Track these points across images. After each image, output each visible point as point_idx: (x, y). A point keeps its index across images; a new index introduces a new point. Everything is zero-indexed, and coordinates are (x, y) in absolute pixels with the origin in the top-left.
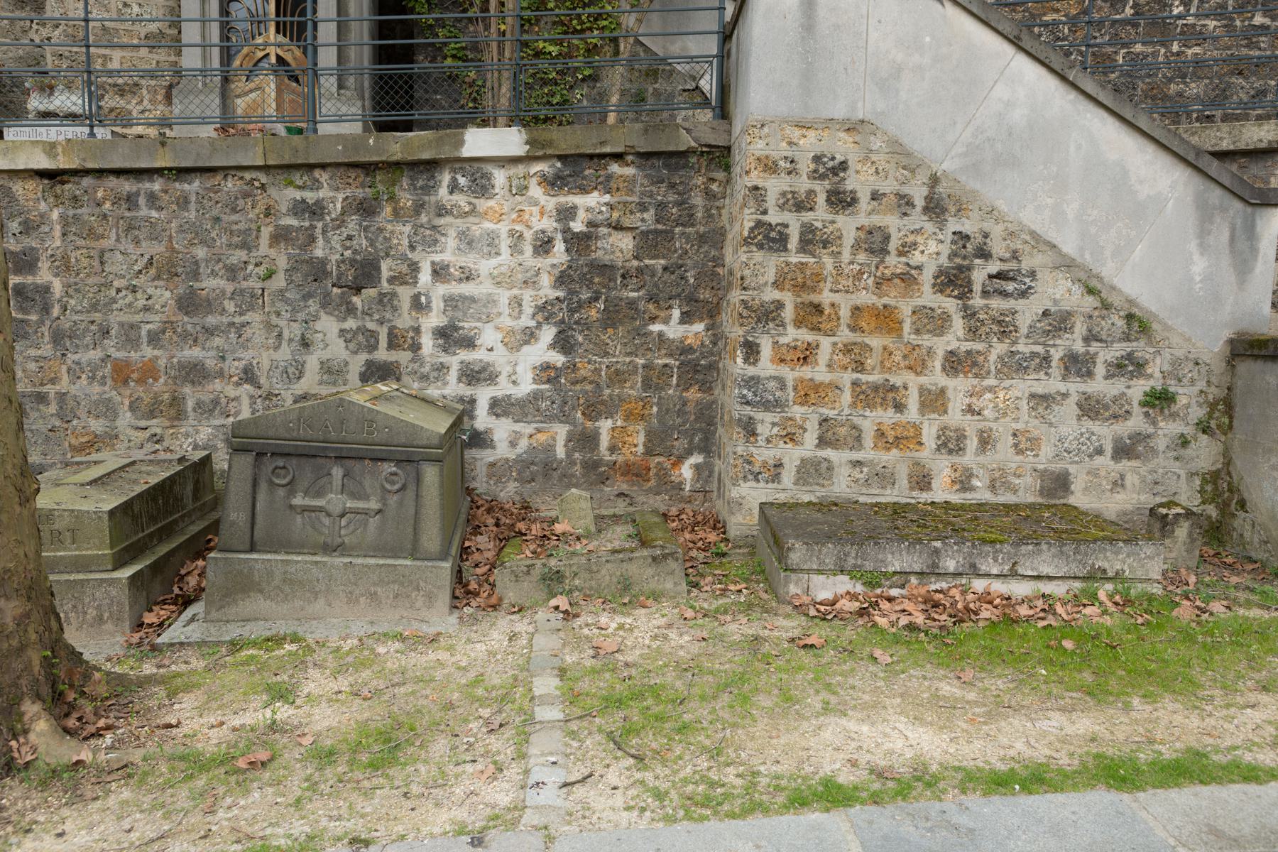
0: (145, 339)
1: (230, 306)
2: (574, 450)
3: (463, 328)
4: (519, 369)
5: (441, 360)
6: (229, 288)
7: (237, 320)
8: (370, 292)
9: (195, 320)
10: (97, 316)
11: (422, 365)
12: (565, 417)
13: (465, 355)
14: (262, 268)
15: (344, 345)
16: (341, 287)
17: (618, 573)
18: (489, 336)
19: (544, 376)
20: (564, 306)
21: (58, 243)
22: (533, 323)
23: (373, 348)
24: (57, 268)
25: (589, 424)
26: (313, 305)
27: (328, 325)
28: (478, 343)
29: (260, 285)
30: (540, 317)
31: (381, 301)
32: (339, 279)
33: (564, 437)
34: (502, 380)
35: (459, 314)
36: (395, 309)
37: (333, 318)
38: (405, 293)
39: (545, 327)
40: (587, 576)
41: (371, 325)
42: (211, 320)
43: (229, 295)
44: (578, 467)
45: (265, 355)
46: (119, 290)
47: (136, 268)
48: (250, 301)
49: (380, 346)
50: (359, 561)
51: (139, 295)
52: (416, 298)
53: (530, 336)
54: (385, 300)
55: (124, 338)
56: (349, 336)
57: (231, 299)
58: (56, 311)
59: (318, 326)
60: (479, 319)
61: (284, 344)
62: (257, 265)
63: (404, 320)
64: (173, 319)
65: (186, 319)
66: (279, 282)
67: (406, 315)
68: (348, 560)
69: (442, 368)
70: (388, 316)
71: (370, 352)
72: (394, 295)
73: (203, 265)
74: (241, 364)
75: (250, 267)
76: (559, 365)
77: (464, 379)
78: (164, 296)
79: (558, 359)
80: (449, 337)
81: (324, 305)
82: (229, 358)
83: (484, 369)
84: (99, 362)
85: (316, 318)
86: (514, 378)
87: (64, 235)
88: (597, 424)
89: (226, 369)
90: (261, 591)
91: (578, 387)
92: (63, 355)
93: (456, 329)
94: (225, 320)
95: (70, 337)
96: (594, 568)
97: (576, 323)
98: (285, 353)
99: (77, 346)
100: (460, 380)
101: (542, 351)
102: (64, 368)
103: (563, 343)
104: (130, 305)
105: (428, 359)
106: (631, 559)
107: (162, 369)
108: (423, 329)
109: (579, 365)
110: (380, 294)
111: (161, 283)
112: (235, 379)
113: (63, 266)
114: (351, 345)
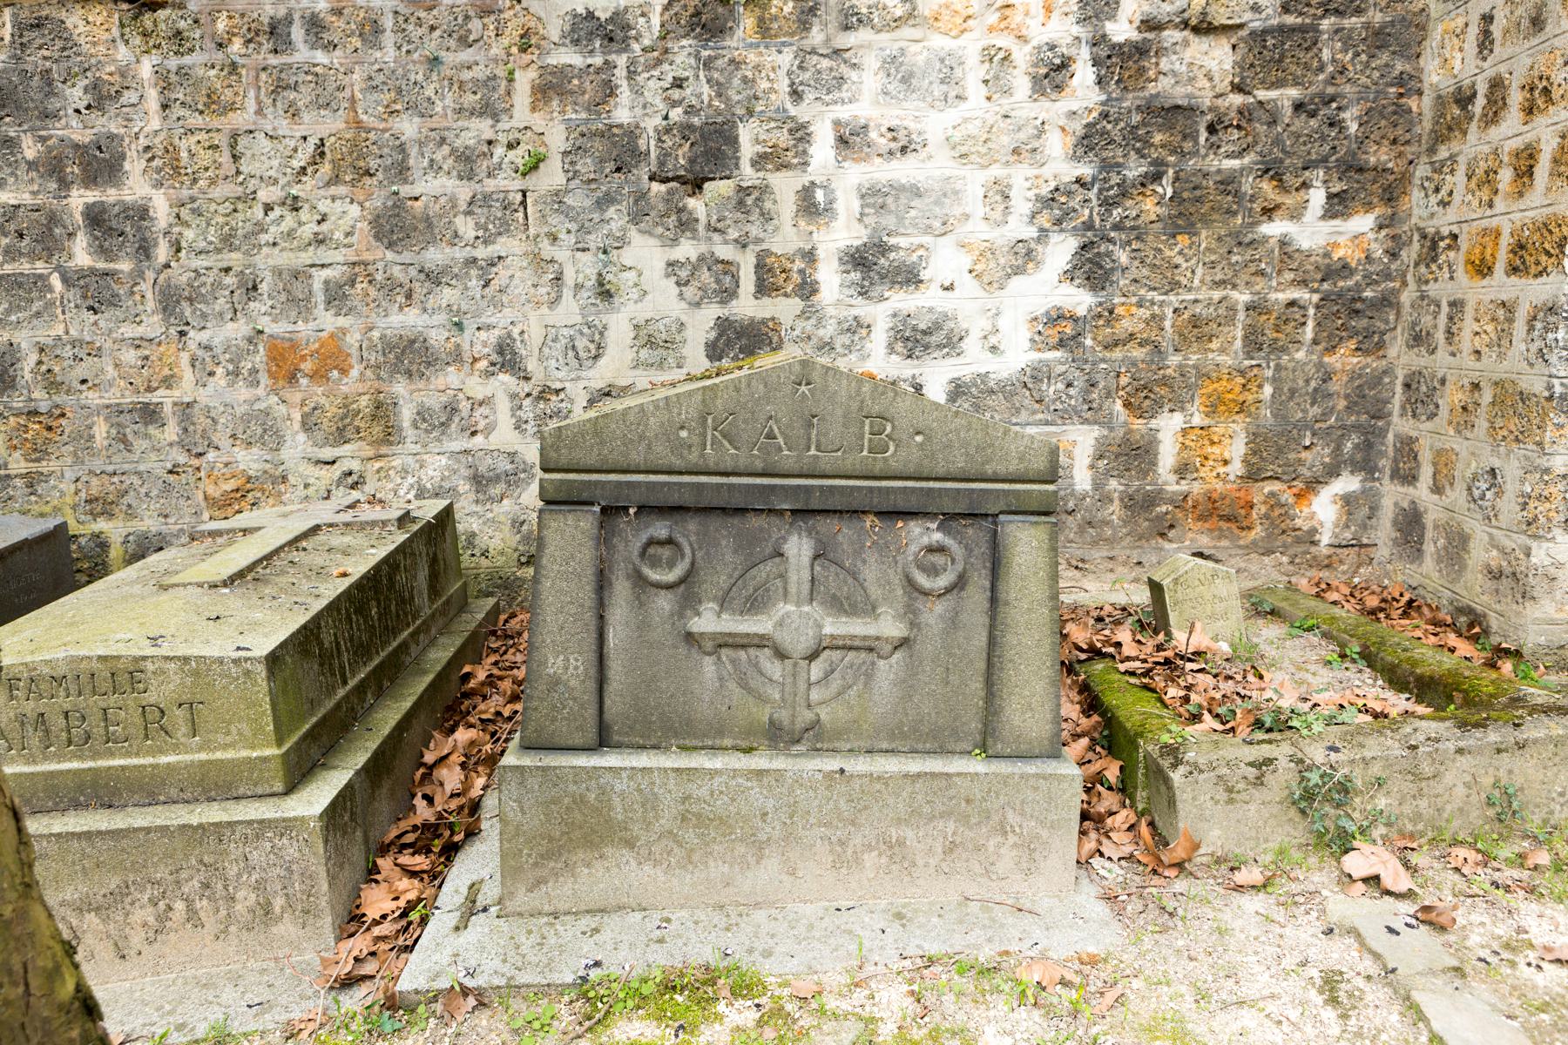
0: (320, 297)
1: (466, 228)
2: (1108, 474)
3: (897, 248)
4: (1002, 323)
5: (855, 312)
6: (464, 192)
7: (482, 253)
8: (718, 189)
9: (407, 257)
10: (234, 259)
11: (819, 324)
12: (1091, 412)
13: (901, 300)
14: (520, 151)
15: (675, 290)
16: (665, 181)
17: (1487, 781)
18: (945, 262)
19: (1053, 334)
20: (1093, 194)
21: (155, 123)
22: (1031, 232)
23: (728, 294)
24: (159, 170)
25: (1138, 424)
26: (616, 217)
27: (646, 254)
28: (924, 275)
29: (518, 184)
30: (1044, 220)
31: (741, 203)
32: (662, 164)
33: (1091, 451)
34: (972, 345)
35: (889, 221)
36: (767, 217)
37: (652, 241)
38: (785, 186)
39: (1055, 238)
40: (1409, 787)
41: (724, 252)
42: (435, 256)
43: (463, 206)
44: (1116, 506)
45: (533, 316)
46: (268, 208)
47: (296, 164)
48: (504, 214)
49: (741, 291)
50: (859, 765)
51: (304, 215)
52: (806, 193)
53: (1025, 257)
54: (749, 201)
55: (283, 297)
56: (684, 274)
57: (468, 213)
58: (162, 252)
59: (627, 256)
60: (928, 230)
61: (567, 293)
62: (510, 146)
63: (785, 239)
64: (367, 256)
65: (390, 255)
66: (552, 176)
67: (788, 229)
68: (832, 764)
69: (858, 327)
70: (754, 231)
71: (723, 302)
72: (765, 189)
73: (413, 151)
74: (492, 337)
75: (499, 151)
76: (1081, 311)
77: (899, 346)
78: (348, 214)
79: (1080, 300)
80: (870, 265)
81: (636, 217)
82: (470, 326)
83: (937, 326)
84: (243, 344)
85: (622, 242)
86: (993, 340)
87: (165, 107)
88: (1154, 423)
89: (466, 346)
90: (630, 844)
91: (1117, 354)
92: (182, 334)
93: (883, 249)
94: (460, 254)
95: (190, 300)
96: (1427, 769)
97: (1117, 227)
98: (569, 311)
99: (204, 316)
100: (891, 349)
101: (1050, 285)
102: (185, 358)
103: (1091, 268)
104: (290, 234)
105: (831, 311)
106: (1521, 746)
107: (354, 352)
108: (821, 253)
109: (1119, 310)
110: (740, 189)
111: (341, 190)
112: (483, 364)
113: (168, 166)
114: (690, 292)
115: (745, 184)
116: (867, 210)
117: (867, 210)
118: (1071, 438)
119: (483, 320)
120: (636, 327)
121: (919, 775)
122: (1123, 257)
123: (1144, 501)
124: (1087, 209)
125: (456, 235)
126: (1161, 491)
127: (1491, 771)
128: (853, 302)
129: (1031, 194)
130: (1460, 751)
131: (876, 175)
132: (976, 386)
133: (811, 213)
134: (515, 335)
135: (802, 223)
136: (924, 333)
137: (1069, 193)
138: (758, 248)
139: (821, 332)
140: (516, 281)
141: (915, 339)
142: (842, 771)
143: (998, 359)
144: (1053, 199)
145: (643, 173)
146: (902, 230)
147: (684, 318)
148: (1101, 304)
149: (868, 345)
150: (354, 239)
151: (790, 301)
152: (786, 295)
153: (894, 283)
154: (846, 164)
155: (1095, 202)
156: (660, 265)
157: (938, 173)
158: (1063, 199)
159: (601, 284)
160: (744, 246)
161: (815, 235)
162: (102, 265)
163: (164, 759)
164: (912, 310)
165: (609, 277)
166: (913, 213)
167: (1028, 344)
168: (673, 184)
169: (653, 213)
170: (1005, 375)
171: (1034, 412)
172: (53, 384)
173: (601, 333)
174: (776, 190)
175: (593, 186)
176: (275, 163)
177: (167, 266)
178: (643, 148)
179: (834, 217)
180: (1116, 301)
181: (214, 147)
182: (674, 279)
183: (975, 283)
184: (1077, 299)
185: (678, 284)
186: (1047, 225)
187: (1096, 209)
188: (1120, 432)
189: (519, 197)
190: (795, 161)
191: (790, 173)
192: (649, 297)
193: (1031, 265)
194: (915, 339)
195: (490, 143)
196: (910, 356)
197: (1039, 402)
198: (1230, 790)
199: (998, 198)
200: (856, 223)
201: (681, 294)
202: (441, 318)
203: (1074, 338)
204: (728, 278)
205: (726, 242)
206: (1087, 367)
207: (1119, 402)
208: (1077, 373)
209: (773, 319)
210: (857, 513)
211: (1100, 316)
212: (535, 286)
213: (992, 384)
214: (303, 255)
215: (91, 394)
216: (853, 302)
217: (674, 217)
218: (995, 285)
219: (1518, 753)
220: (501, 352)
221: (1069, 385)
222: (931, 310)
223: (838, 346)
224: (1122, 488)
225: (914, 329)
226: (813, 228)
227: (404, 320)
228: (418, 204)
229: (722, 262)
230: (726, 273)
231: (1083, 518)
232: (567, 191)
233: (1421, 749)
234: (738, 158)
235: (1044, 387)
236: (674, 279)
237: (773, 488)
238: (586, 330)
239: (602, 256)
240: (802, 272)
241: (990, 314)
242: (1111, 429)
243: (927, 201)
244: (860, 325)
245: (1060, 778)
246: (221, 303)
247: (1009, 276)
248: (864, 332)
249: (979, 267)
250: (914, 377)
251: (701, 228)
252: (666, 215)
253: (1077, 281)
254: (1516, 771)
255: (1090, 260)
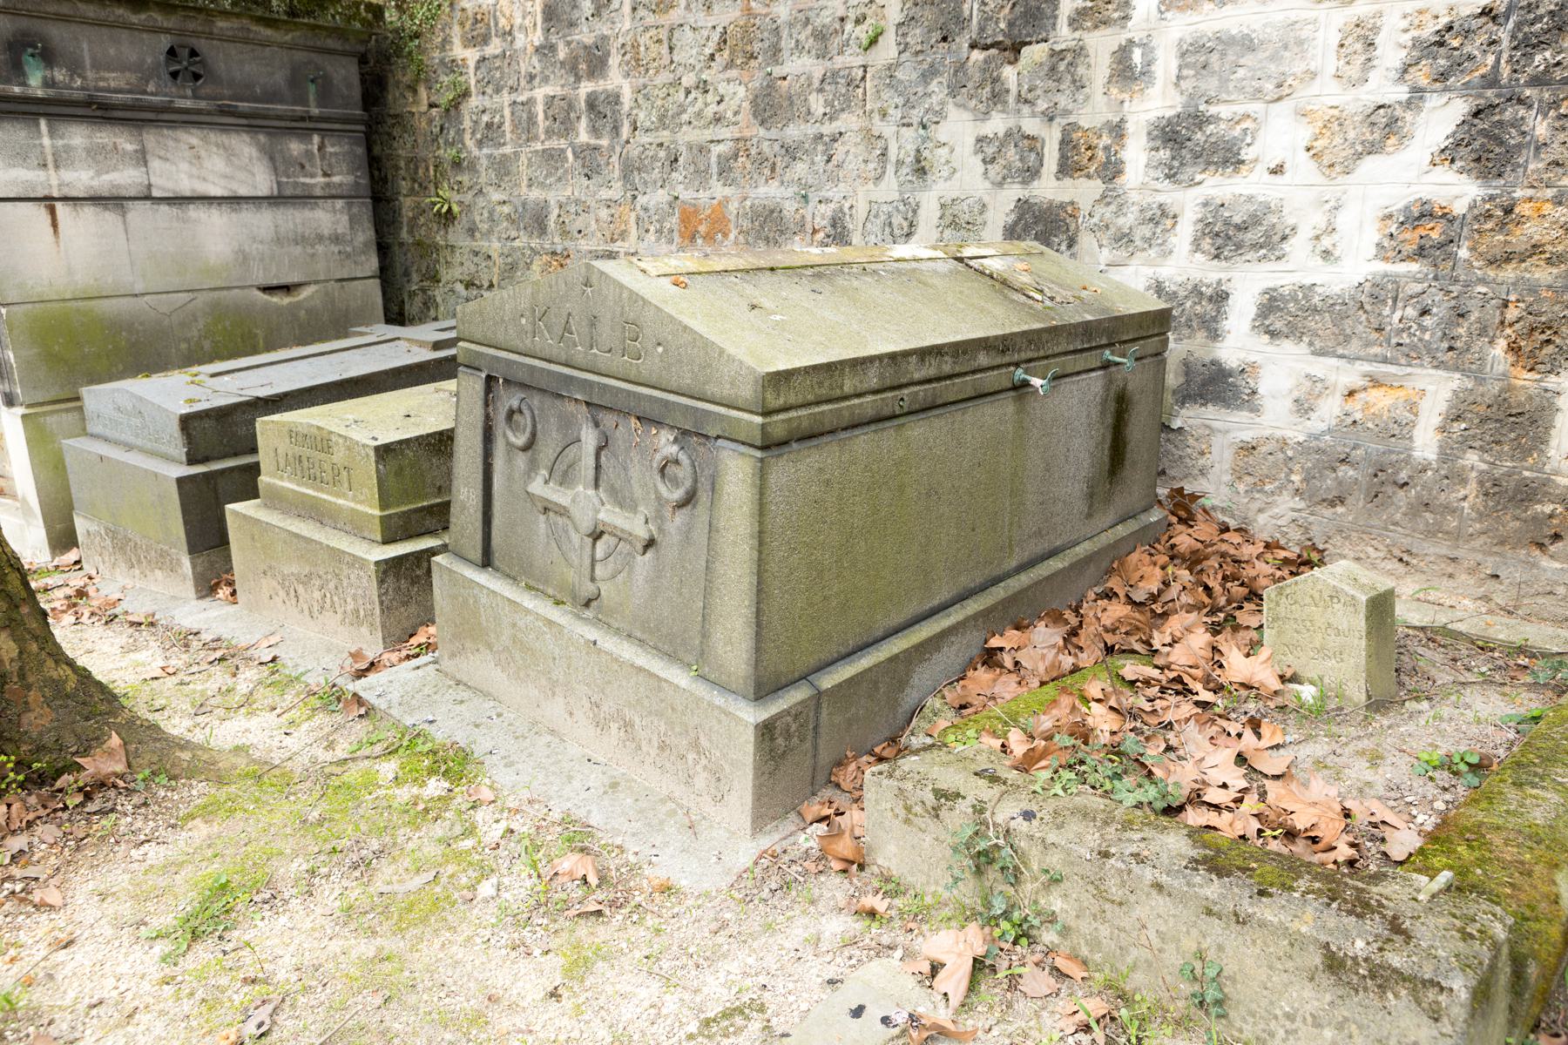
0: (714, 169)
1: (817, 104)
2: (1466, 443)
3: (1216, 119)
4: (1343, 220)
5: (1161, 198)
6: (817, 69)
7: (828, 129)
8: (1034, 53)
9: (774, 133)
10: (664, 136)
11: (1119, 212)
12: (1452, 354)
13: (1217, 186)
14: (864, 27)
15: (980, 168)
16: (986, 48)
17: (1189, 945)
18: (1279, 136)
19: (1411, 237)
20: (1504, 34)
21: (627, 25)
22: (1401, 93)
23: (1031, 174)
24: (628, 63)
25: (1525, 380)
26: (938, 88)
27: (960, 129)
28: (1247, 154)
29: (860, 61)
30: (1421, 76)
31: (1053, 69)
32: (982, 29)
33: (1443, 407)
34: (1298, 248)
35: (1210, 85)
36: (1078, 85)
37: (967, 115)
38: (1101, 44)
39: (1433, 101)
40: (1087, 900)
41: (1031, 126)
42: (795, 132)
43: (816, 84)
44: (1471, 489)
45: (861, 191)
46: (688, 92)
47: (708, 51)
48: (845, 89)
49: (1044, 170)
50: (609, 643)
51: (710, 97)
52: (1122, 53)
53: (1386, 127)
54: (1062, 67)
55: (692, 169)
56: (990, 150)
57: (821, 90)
58: (625, 130)
59: (942, 133)
60: (1257, 94)
61: (890, 169)
62: (858, 22)
63: (1093, 113)
64: (747, 134)
65: (762, 132)
66: (888, 50)
67: (1099, 98)
68: (591, 633)
69: (1161, 217)
70: (1063, 101)
71: (1024, 182)
72: (1079, 52)
73: (785, 34)
74: (827, 210)
75: (849, 27)
76: (1459, 208)
77: (1206, 244)
78: (737, 92)
79: (1460, 191)
80: (1182, 142)
81: (953, 93)
82: (814, 198)
83: (1254, 220)
84: (666, 207)
85: (940, 115)
86: (1326, 242)
87: (634, 9)
88: (1552, 382)
89: (809, 218)
90: (490, 647)
91: (1509, 273)
92: (634, 197)
93: (1200, 121)
94: (811, 130)
95: (639, 170)
96: (1114, 889)
97: (1537, 81)
98: (889, 189)
99: (645, 183)
100: (1196, 246)
101: (1420, 169)
102: (633, 215)
103: (1485, 146)
104: (699, 114)
105: (1134, 196)
106: (1241, 920)
107: (732, 218)
108: (1130, 127)
109: (1523, 209)
110: (1053, 53)
111: (734, 73)
112: (820, 236)
114: (994, 170)
115: (1058, 48)
116: (1185, 72)
117: (1185, 72)
118: (1420, 385)
119: (824, 194)
120: (943, 206)
121: (640, 669)
122: (1541, 128)
123: (1517, 490)
124: (1490, 56)
125: (809, 113)
126: (1546, 483)
127: (1194, 932)
128: (1159, 186)
129: (1406, 39)
130: (1159, 887)
131: (1202, 27)
132: (1296, 301)
133: (1126, 78)
134: (846, 210)
135: (1114, 91)
136: (1238, 228)
137: (1467, 33)
138: (1064, 122)
139: (1121, 221)
140: (850, 157)
141: (1227, 235)
142: (595, 643)
143: (1331, 269)
144: (1441, 44)
145: (963, 42)
146: (1224, 96)
147: (986, 199)
148: (1492, 198)
149: (1173, 240)
150: (739, 118)
151: (1091, 183)
152: (1089, 177)
153: (1209, 163)
154: (1168, 15)
155: (1505, 44)
156: (971, 141)
157: (1280, 17)
158: (1455, 43)
159: (918, 161)
160: (1051, 119)
161: (1126, 104)
162: (593, 142)
163: (341, 502)
164: (1227, 199)
165: (926, 154)
166: (1241, 72)
167: (1373, 251)
168: (993, 51)
169: (970, 85)
170: (1336, 290)
171: (1368, 344)
172: (565, 234)
173: (915, 212)
174: (1091, 52)
175: (920, 58)
176: (694, 52)
177: (628, 142)
178: (966, 13)
179: (1151, 83)
180: (1518, 194)
181: (659, 41)
182: (980, 156)
183: (1312, 165)
184: (1455, 191)
185: (984, 161)
186: (1424, 82)
187: (1505, 56)
188: (1495, 388)
189: (860, 73)
190: (1116, 15)
191: (1109, 31)
192: (957, 175)
193: (1393, 140)
194: (1227, 235)
195: (842, 20)
196: (1217, 257)
197: (1379, 330)
198: (908, 809)
199: (1359, 46)
200: (1172, 87)
201: (986, 172)
202: (790, 192)
203: (1441, 246)
204: (1033, 156)
205: (1033, 115)
206: (1456, 289)
207: (1502, 344)
208: (1439, 296)
209: (1072, 203)
210: (624, 413)
211: (1488, 216)
212: (866, 162)
213: (1316, 300)
214: (706, 132)
215: (582, 242)
216: (1159, 186)
217: (988, 89)
218: (1338, 168)
219: (1233, 925)
220: (834, 226)
221: (1425, 312)
222: (1250, 199)
223: (1137, 239)
224: (1484, 467)
225: (1227, 223)
226: (1126, 96)
227: (769, 191)
228: (786, 83)
229: (1028, 137)
230: (1031, 150)
231: (1418, 496)
232: (898, 65)
233: (1112, 861)
234: (1056, 17)
235: (1387, 311)
236: (980, 156)
237: (571, 378)
238: (901, 208)
239: (921, 132)
240: (1107, 148)
241: (1327, 207)
242: (1480, 381)
243: (1261, 55)
244: (1164, 214)
245: (739, 720)
246: (656, 174)
247: (1359, 156)
248: (1169, 222)
249: (1319, 144)
250: (1219, 282)
251: (1011, 99)
252: (981, 86)
253: (1459, 164)
254: (1229, 951)
255: (1483, 132)
